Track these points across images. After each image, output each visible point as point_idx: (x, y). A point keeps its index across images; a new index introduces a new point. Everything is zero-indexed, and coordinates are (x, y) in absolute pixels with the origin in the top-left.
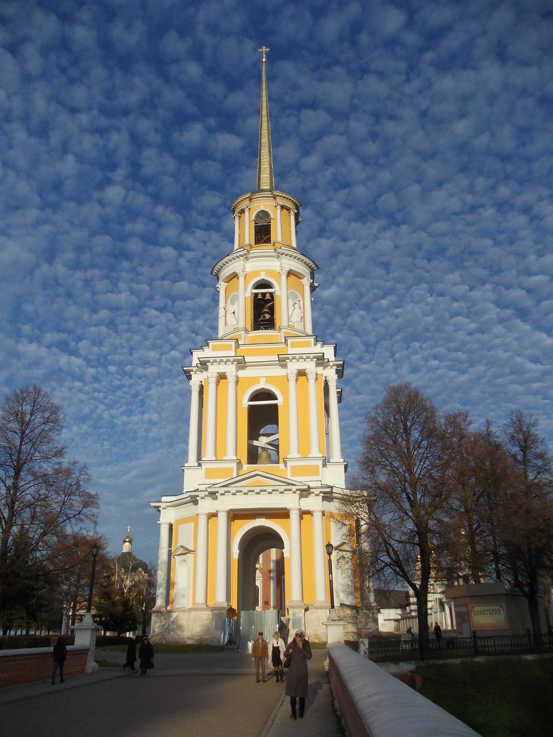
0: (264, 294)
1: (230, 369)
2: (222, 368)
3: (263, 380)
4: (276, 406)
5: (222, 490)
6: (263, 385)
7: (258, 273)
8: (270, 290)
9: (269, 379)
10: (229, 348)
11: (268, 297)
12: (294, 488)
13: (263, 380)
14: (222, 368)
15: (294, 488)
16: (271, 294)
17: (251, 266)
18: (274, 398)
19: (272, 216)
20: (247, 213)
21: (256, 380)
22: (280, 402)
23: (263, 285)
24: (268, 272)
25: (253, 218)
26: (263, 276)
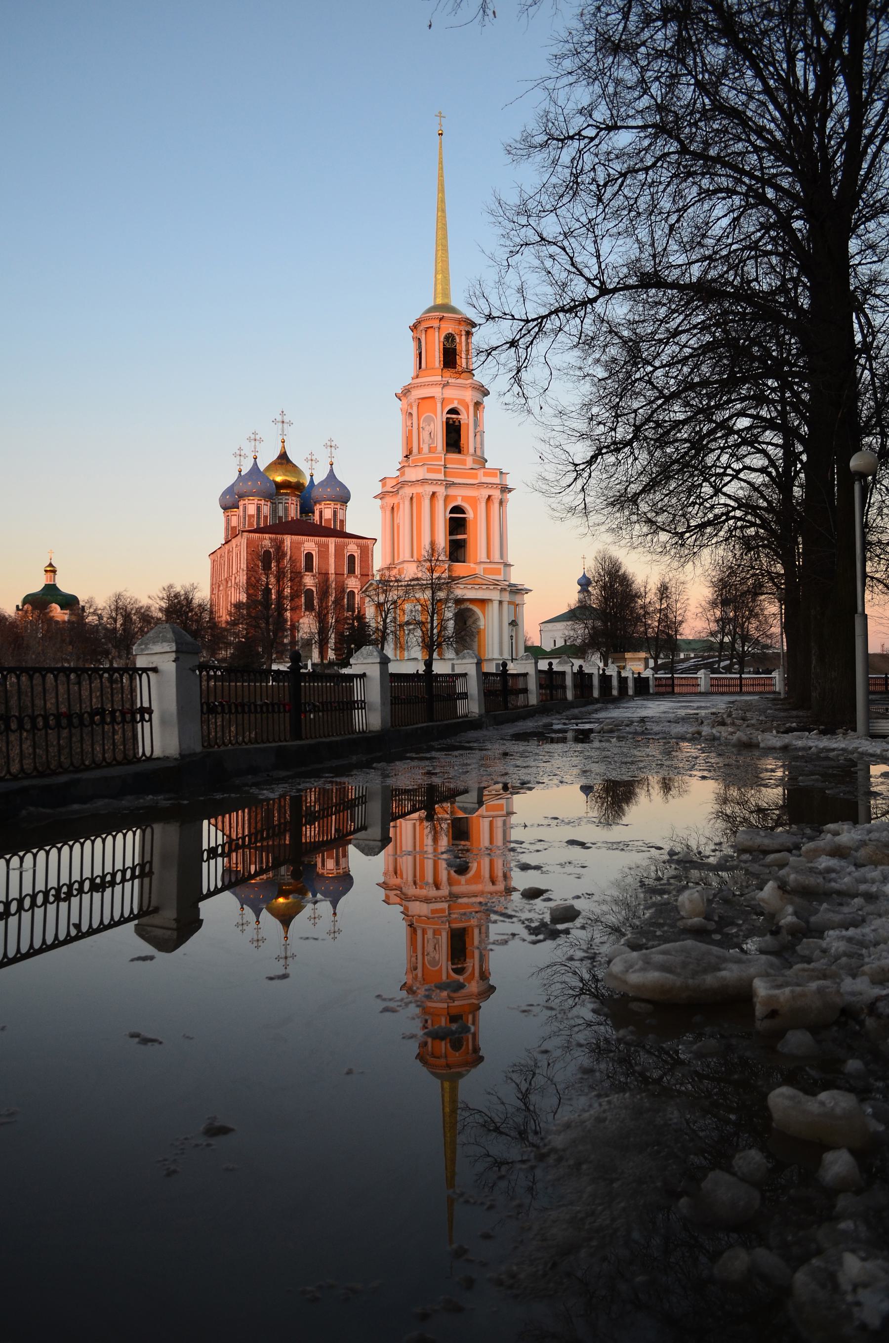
1: (441, 491)
3: (460, 499)
6: (459, 502)
7: (452, 400)
9: (464, 498)
10: (439, 472)
11: (457, 424)
12: (499, 587)
13: (460, 499)
15: (499, 587)
17: (449, 393)
19: (458, 340)
21: (455, 497)
24: (462, 401)
25: (442, 340)
26: (455, 405)
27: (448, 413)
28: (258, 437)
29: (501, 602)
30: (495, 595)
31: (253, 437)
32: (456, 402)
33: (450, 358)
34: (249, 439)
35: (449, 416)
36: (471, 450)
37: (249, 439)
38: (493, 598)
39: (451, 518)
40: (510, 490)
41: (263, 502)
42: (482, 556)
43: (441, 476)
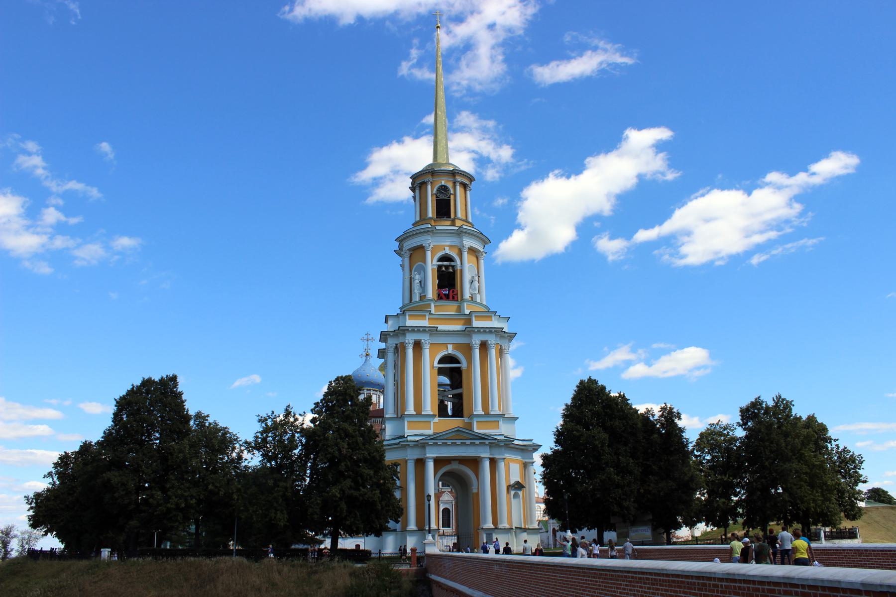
0: (447, 267)
2: (417, 337)
4: (459, 368)
5: (431, 442)
8: (453, 263)
12: (487, 442)
13: (450, 347)
14: (417, 337)
16: (453, 267)
18: (458, 362)
19: (452, 192)
20: (429, 187)
22: (464, 365)
23: (446, 258)
26: (448, 251)
27: (440, 260)
28: (370, 337)
29: (493, 462)
30: (484, 453)
31: (366, 337)
32: (447, 249)
33: (444, 209)
34: (363, 339)
35: (440, 263)
36: (467, 295)
37: (363, 339)
38: (482, 455)
39: (439, 369)
40: (511, 336)
41: (372, 392)
42: (479, 410)
43: (425, 323)
